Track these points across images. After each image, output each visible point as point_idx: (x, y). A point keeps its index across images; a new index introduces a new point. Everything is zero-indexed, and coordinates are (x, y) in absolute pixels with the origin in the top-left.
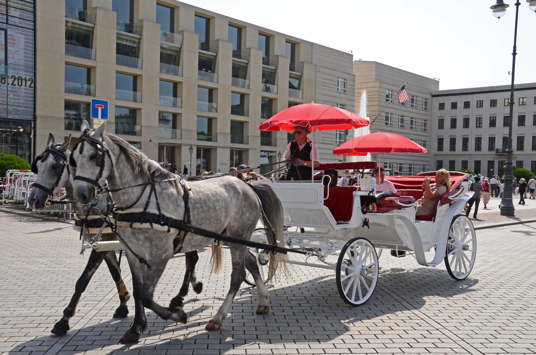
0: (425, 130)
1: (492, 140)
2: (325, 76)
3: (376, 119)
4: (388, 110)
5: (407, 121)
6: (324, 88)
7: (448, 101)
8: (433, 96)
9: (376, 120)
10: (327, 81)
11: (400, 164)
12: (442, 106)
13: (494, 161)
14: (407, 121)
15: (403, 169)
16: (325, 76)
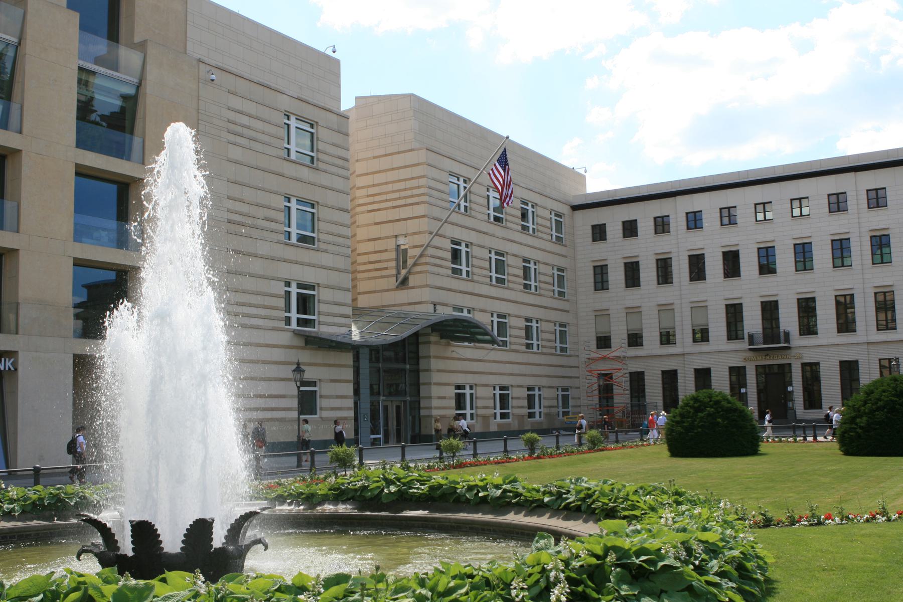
0: (561, 294)
1: (734, 312)
2: (236, 103)
3: (421, 256)
4: (458, 234)
5: (514, 267)
6: (232, 138)
7: (613, 219)
8: (575, 208)
9: (423, 260)
10: (245, 120)
11: (501, 388)
12: (599, 233)
13: (745, 367)
14: (514, 267)
15: (512, 403)
16: (236, 103)
